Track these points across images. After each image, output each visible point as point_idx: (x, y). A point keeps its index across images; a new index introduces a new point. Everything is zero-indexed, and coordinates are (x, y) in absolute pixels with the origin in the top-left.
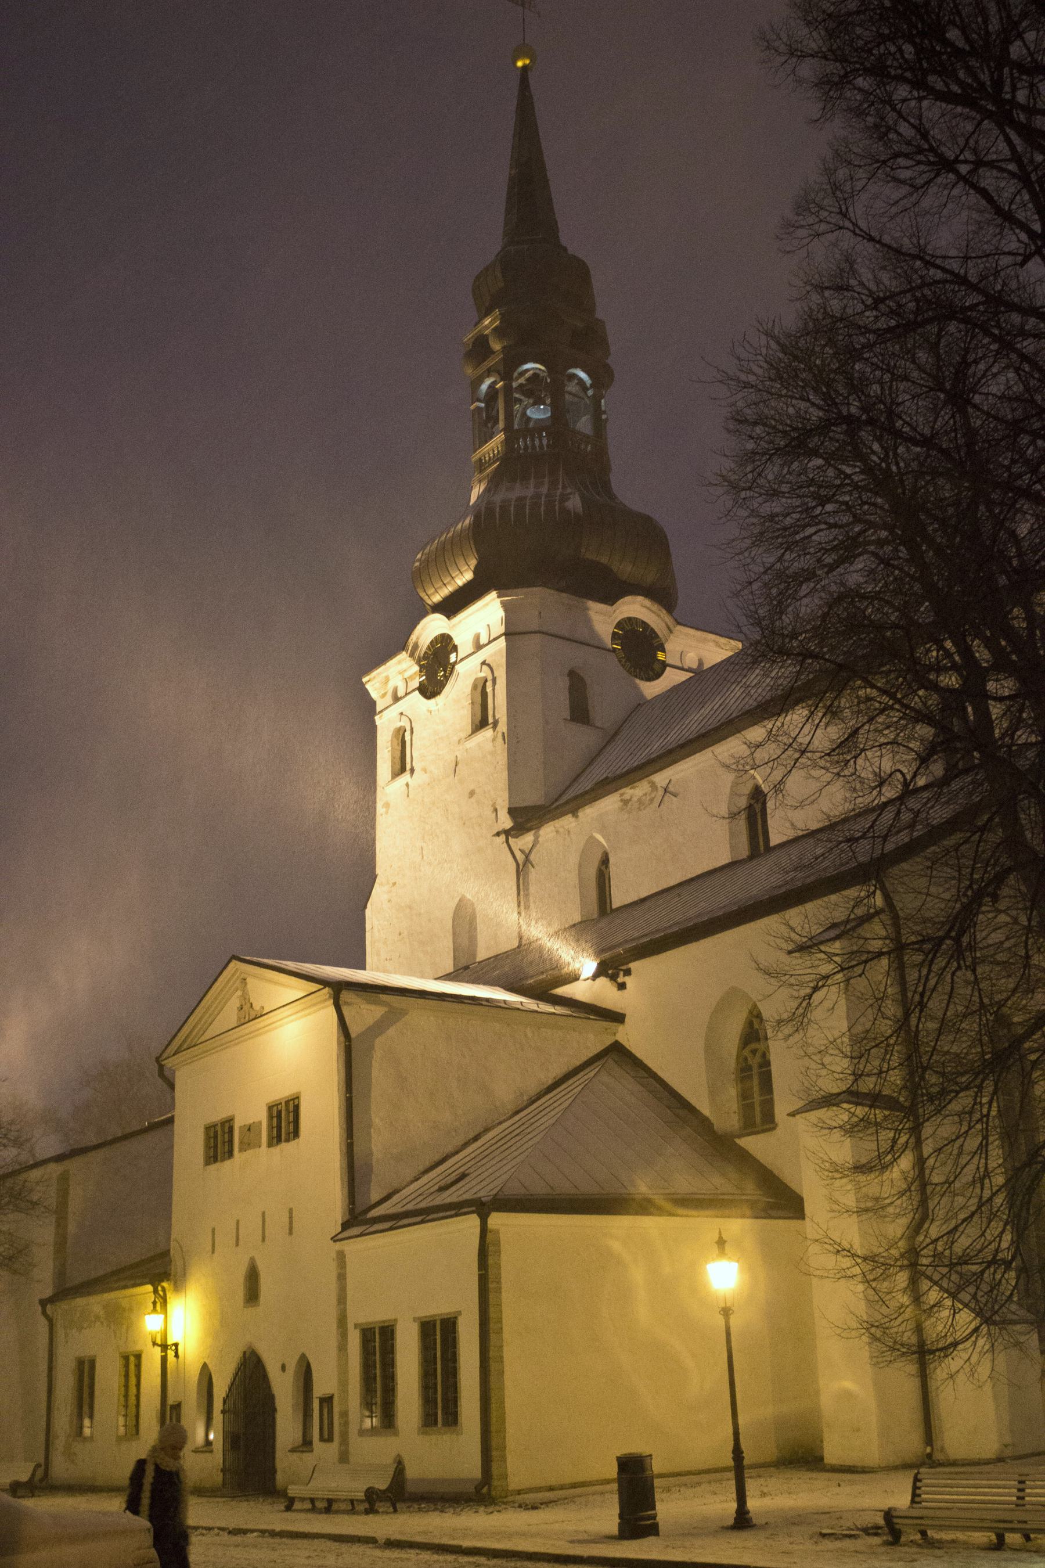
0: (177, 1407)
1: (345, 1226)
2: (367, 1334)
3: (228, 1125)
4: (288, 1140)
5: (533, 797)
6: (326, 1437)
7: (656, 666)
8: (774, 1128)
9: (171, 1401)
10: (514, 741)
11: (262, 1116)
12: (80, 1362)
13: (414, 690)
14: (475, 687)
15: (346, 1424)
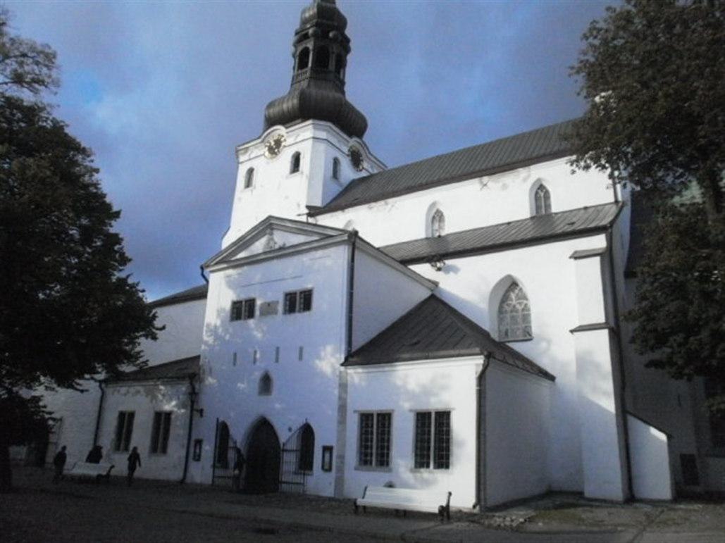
0: (199, 442)
1: (346, 359)
2: (366, 418)
3: (251, 303)
4: (299, 312)
5: (318, 203)
6: (326, 467)
7: (361, 167)
8: (531, 340)
9: (194, 438)
10: (311, 178)
11: (281, 299)
12: (122, 415)
13: (261, 155)
14: (293, 156)
15: (342, 462)
